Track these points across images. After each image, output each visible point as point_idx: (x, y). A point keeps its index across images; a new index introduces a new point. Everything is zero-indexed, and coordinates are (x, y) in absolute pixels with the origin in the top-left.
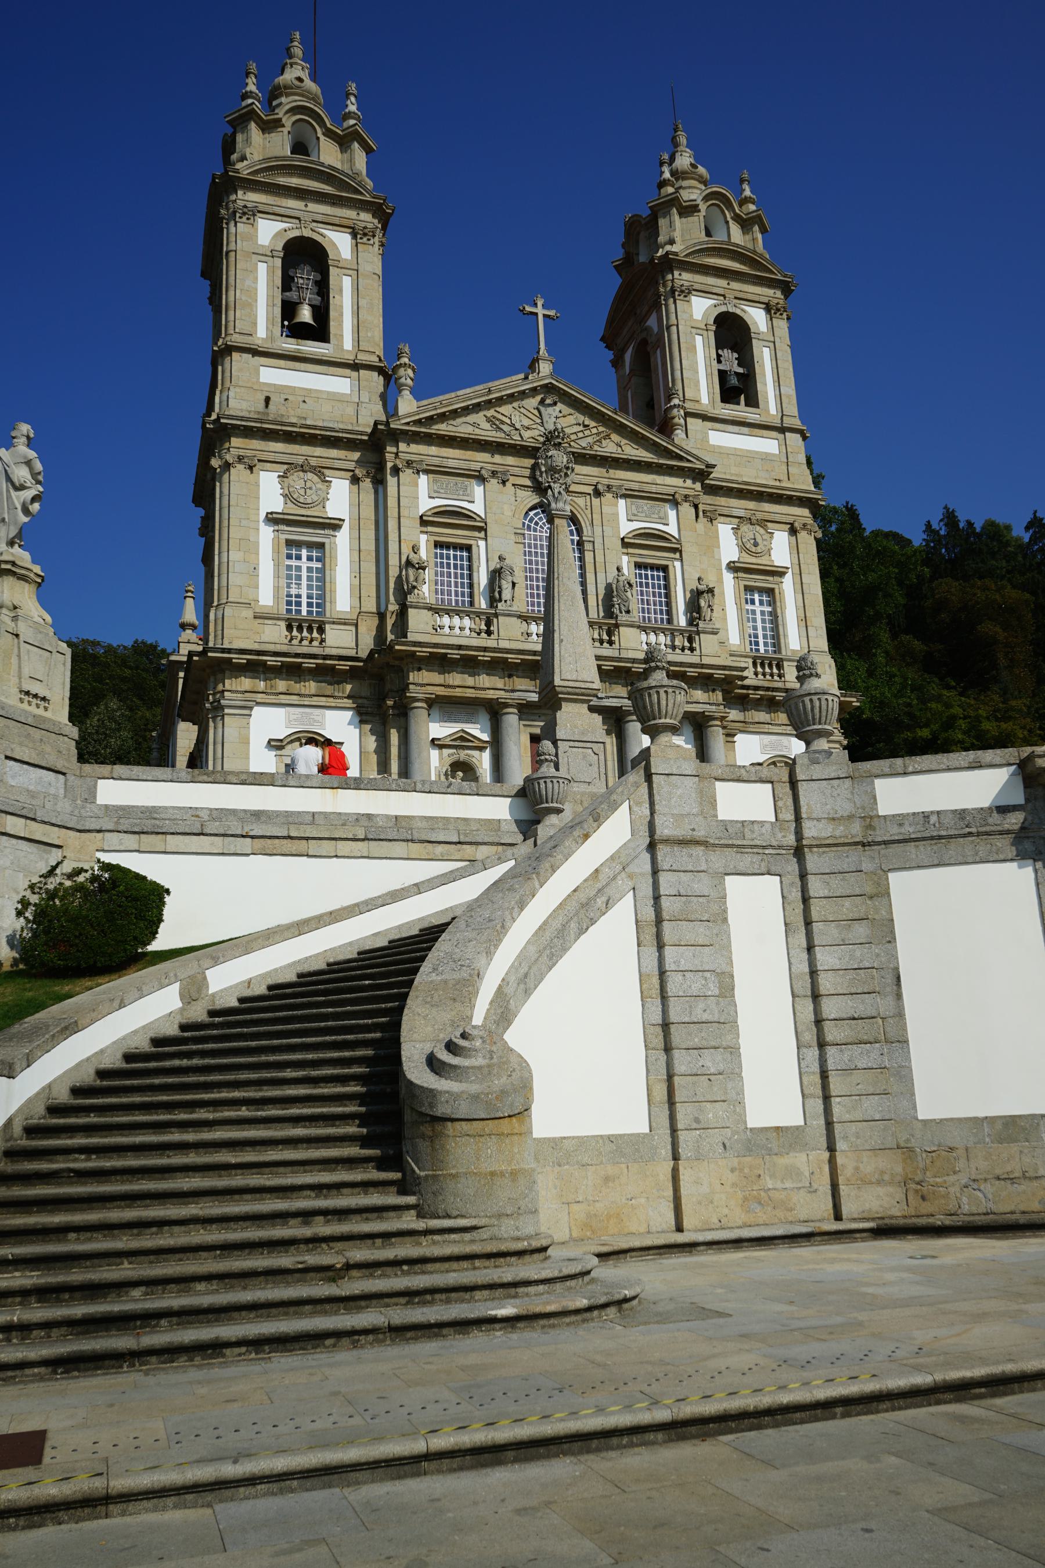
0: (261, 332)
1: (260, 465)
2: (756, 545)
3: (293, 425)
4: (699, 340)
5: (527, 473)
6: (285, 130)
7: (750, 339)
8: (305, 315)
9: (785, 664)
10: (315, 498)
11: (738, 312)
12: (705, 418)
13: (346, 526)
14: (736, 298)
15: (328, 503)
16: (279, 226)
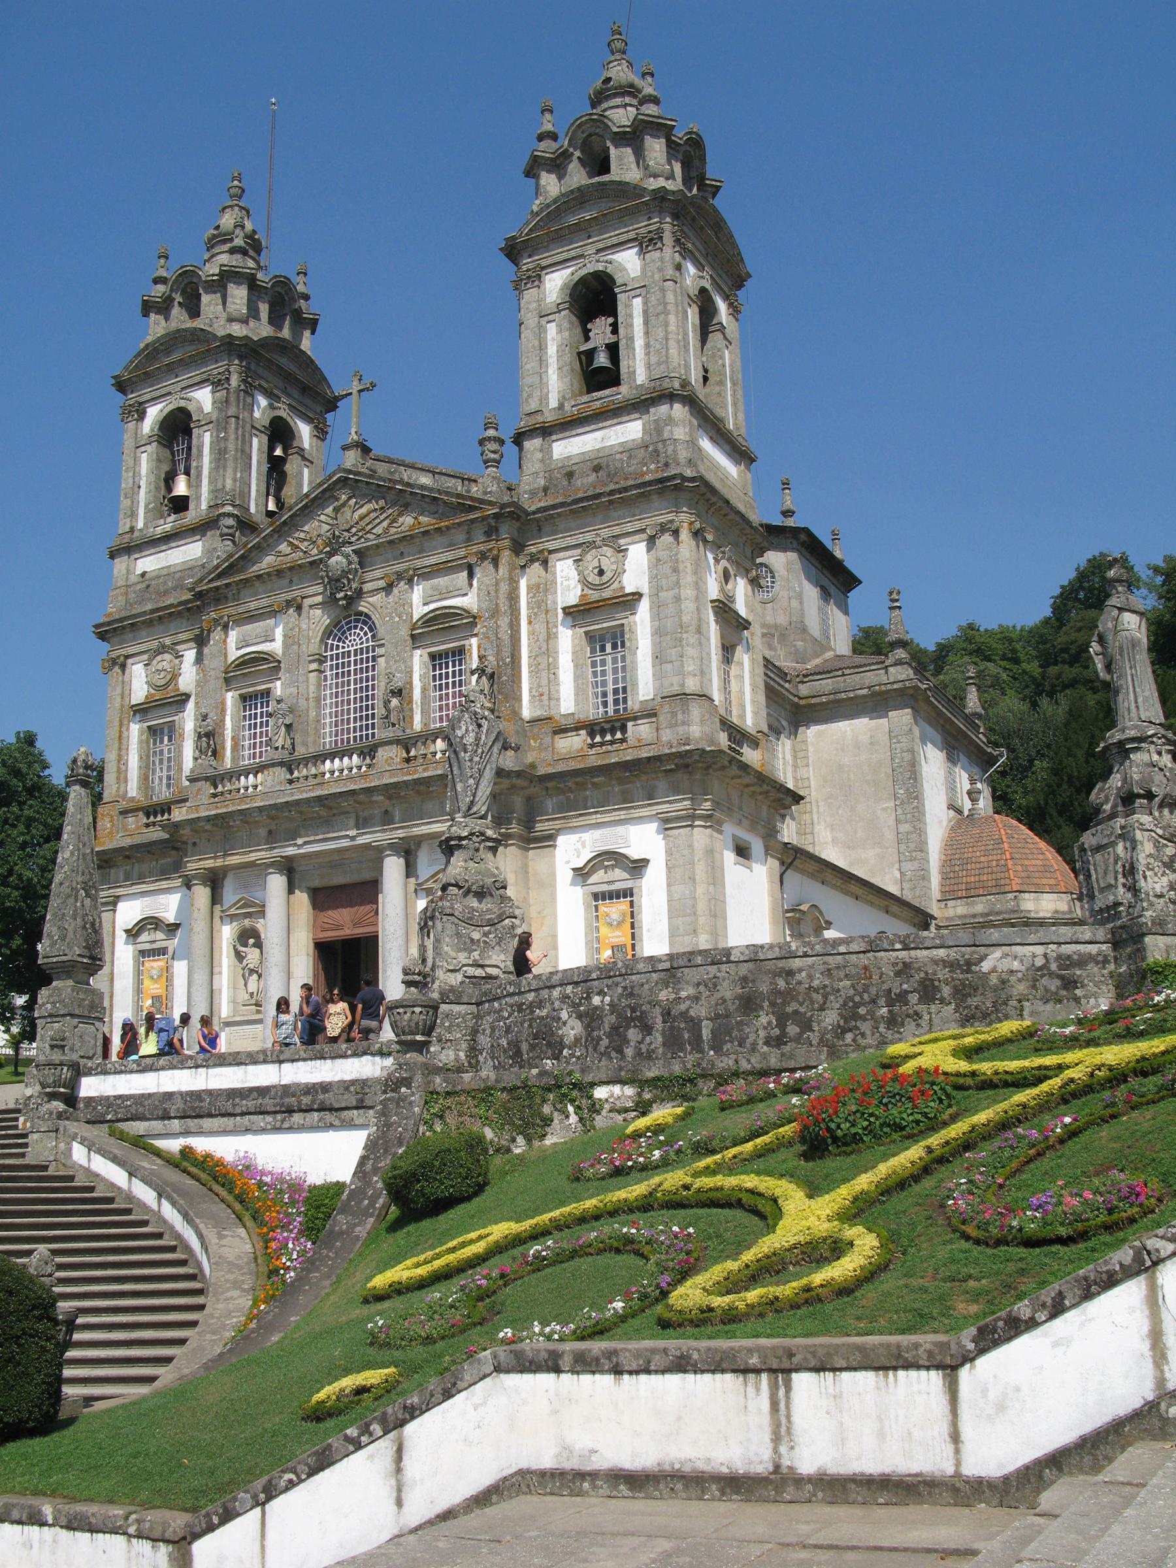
0: (140, 525)
1: (130, 661)
2: (601, 573)
3: (144, 613)
4: (552, 329)
5: (320, 589)
6: (176, 303)
7: (615, 295)
8: (181, 488)
9: (630, 724)
10: (169, 677)
11: (600, 267)
12: (547, 431)
13: (192, 699)
14: (598, 251)
15: (180, 679)
16: (160, 406)
